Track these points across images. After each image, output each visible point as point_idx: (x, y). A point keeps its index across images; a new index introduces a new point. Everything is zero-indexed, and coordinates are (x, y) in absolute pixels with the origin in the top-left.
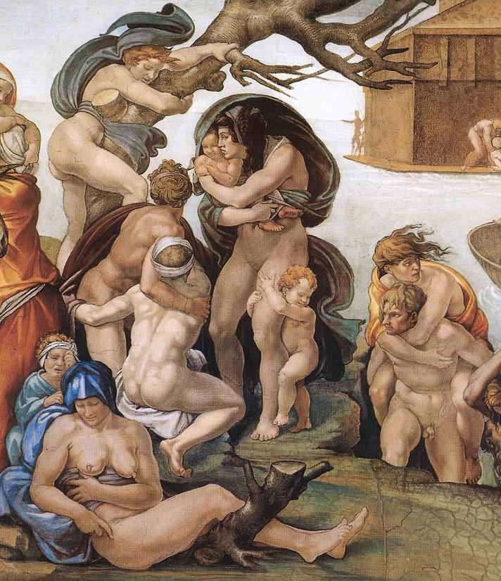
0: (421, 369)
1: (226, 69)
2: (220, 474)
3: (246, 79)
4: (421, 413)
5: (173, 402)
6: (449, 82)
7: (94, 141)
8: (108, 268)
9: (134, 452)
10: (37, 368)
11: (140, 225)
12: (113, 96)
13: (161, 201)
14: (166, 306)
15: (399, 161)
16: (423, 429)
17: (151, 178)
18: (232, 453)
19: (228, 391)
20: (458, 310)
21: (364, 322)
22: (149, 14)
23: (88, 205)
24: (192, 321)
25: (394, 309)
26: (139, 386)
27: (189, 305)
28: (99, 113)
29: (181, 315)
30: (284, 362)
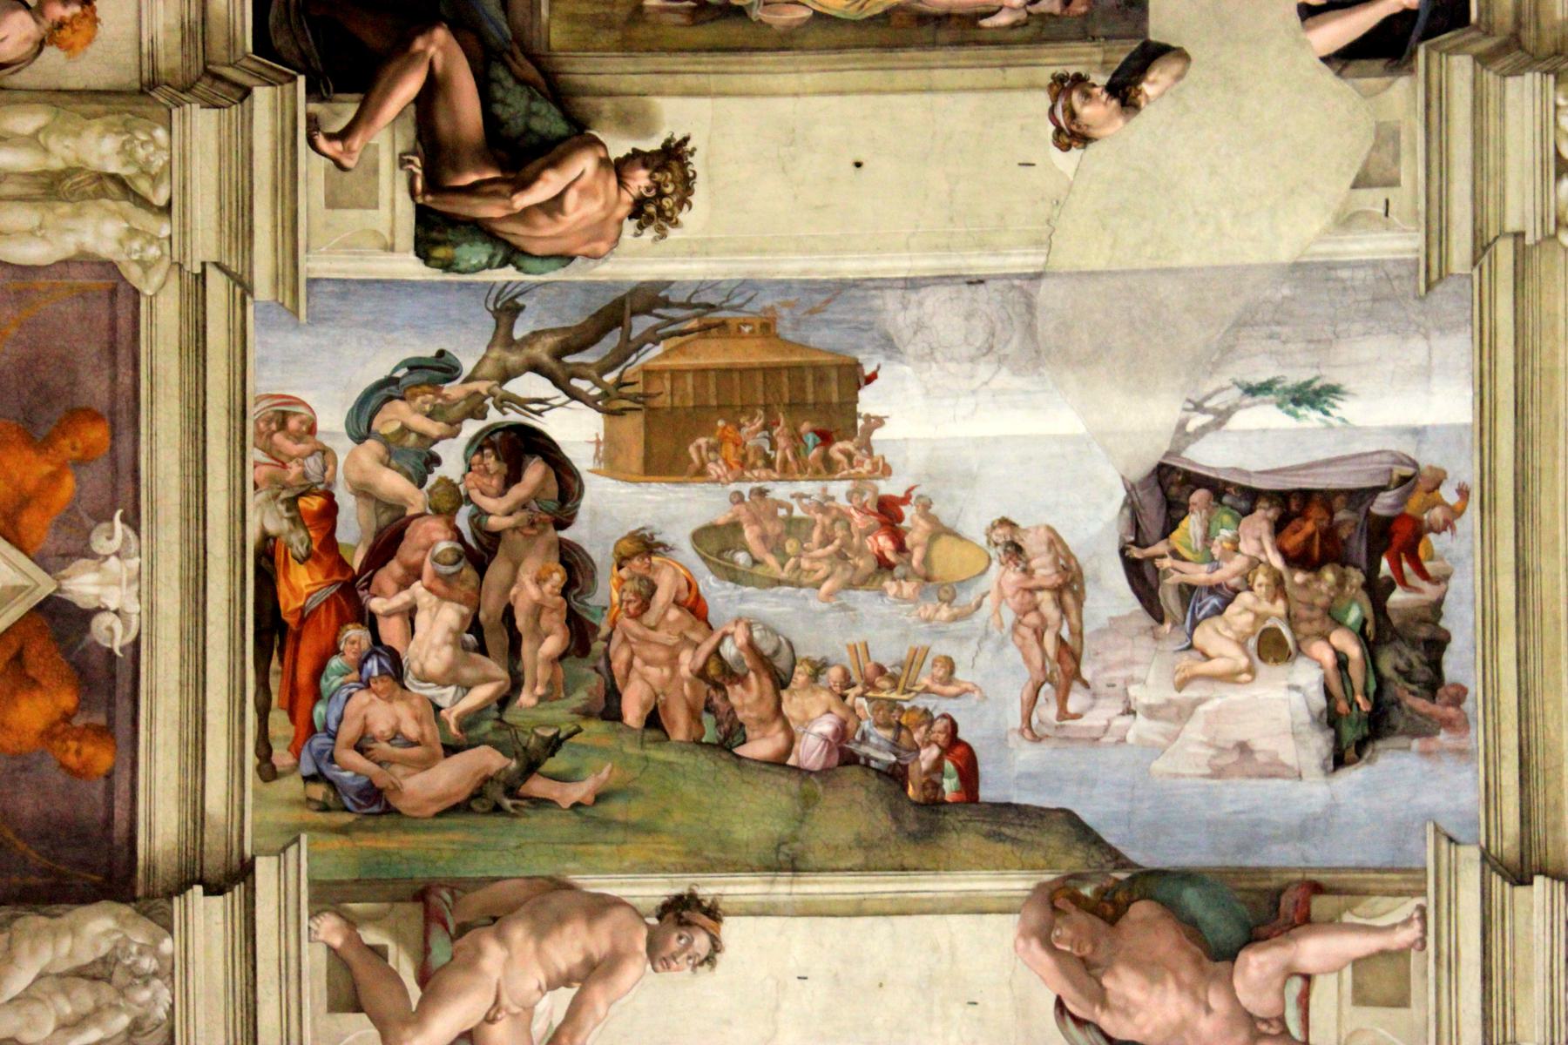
0: (653, 647)
1: (489, 402)
2: (491, 737)
3: (506, 409)
4: (654, 682)
5: (450, 678)
6: (673, 408)
7: (381, 462)
8: (395, 568)
9: (419, 720)
10: (335, 650)
11: (420, 532)
12: (397, 425)
13: (438, 512)
14: (443, 598)
15: (632, 473)
16: (657, 696)
17: (430, 492)
18: (500, 720)
19: (496, 668)
20: (684, 596)
21: (605, 608)
22: (425, 359)
23: (377, 517)
24: (465, 610)
25: (632, 598)
26: (422, 665)
27: (462, 597)
28: (384, 440)
29: (456, 606)
30: (541, 642)
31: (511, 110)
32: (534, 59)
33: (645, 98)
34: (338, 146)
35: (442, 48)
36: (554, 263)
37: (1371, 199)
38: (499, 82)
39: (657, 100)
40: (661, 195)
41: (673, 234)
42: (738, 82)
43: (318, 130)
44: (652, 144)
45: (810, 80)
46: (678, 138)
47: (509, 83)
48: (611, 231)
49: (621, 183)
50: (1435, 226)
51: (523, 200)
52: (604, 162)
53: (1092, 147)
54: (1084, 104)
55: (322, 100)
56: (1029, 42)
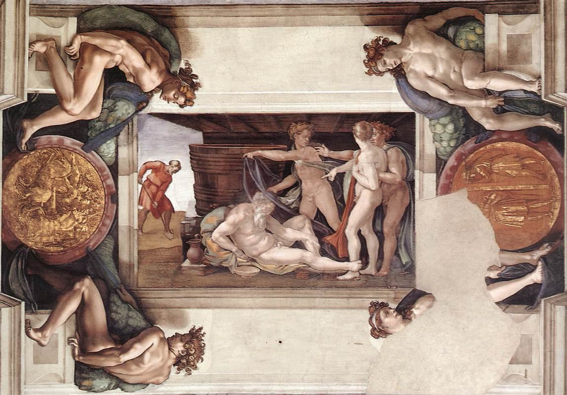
31: (120, 316)
32: (130, 292)
33: (182, 309)
34: (39, 334)
35: (87, 287)
36: (139, 387)
37: (519, 369)
38: (114, 303)
39: (188, 310)
40: (189, 355)
41: (194, 372)
42: (225, 301)
43: (31, 327)
44: (185, 331)
45: (259, 301)
46: (197, 328)
47: (119, 303)
48: (166, 372)
49: (170, 349)
50: (548, 384)
51: (125, 358)
52: (163, 340)
53: (389, 337)
54: (386, 317)
55: (33, 313)
56: (361, 287)
